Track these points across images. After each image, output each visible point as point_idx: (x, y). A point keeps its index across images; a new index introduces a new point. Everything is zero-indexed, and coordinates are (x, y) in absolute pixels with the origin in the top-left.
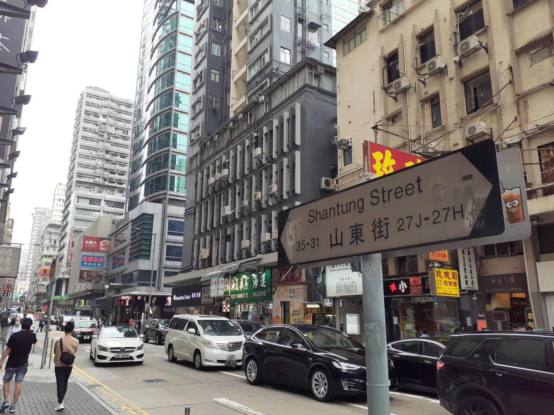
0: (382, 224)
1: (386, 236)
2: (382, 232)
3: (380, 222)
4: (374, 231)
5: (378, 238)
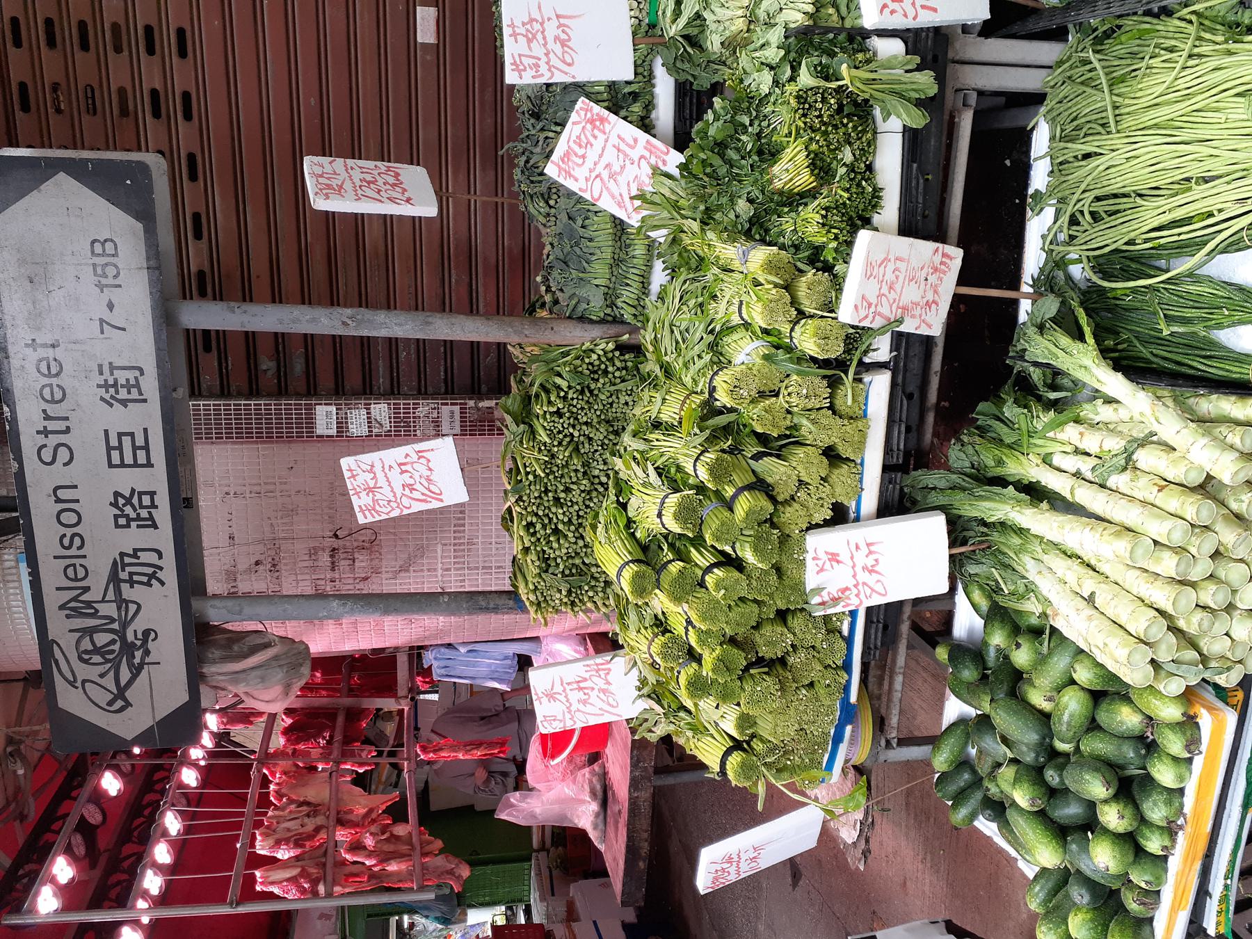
2: (128, 380)
3: (106, 386)
4: (124, 403)
5: (141, 394)
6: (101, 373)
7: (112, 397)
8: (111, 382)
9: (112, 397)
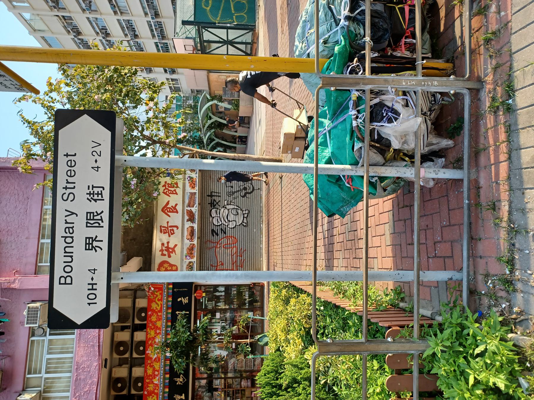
0: (92, 192)
1: (102, 189)
3: (90, 194)
4: (95, 200)
5: (102, 197)
6: (89, 189)
7: (91, 198)
8: (92, 192)
9: (91, 198)
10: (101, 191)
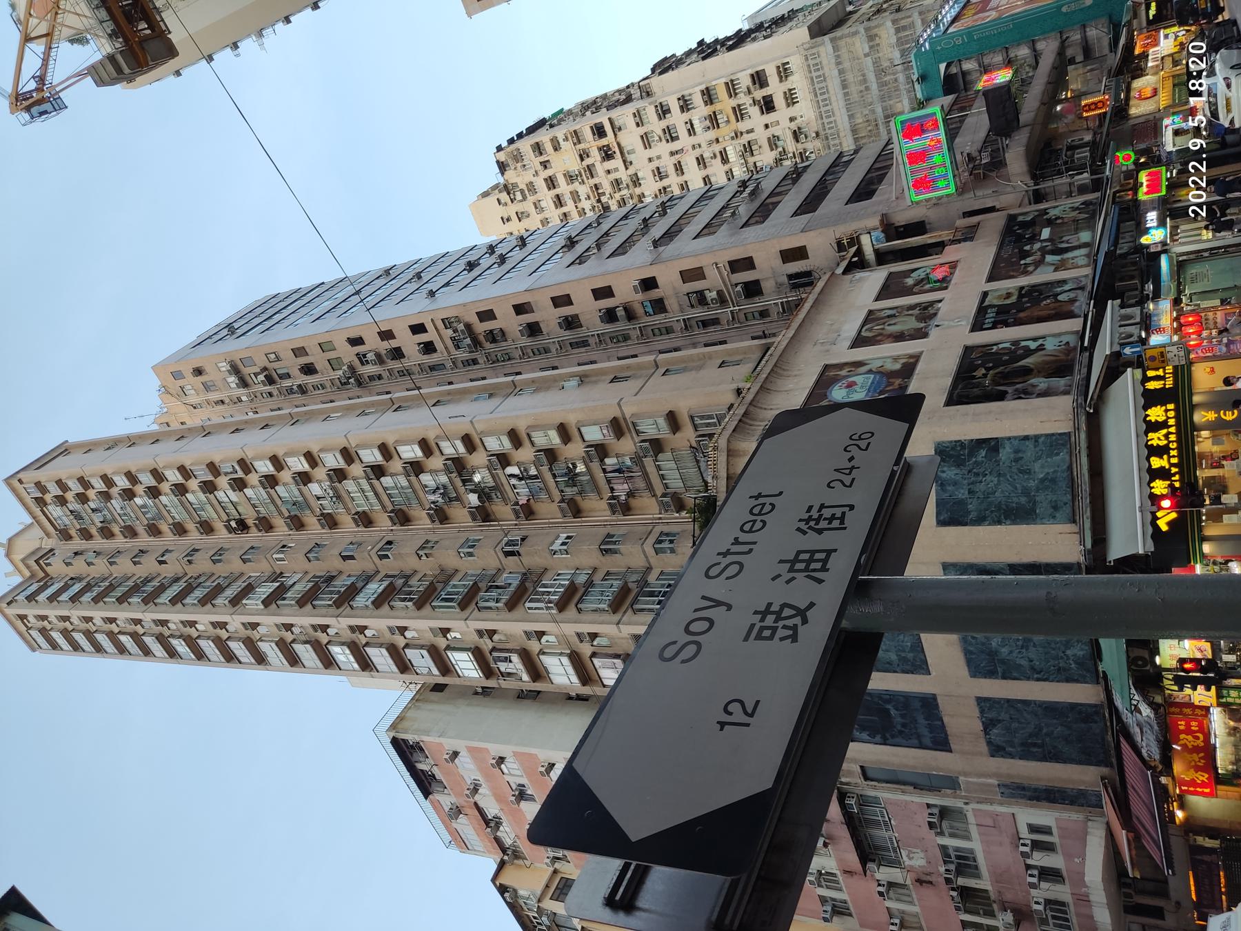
4: (820, 532)
8: (816, 516)
9: (810, 528)
10: (844, 514)
